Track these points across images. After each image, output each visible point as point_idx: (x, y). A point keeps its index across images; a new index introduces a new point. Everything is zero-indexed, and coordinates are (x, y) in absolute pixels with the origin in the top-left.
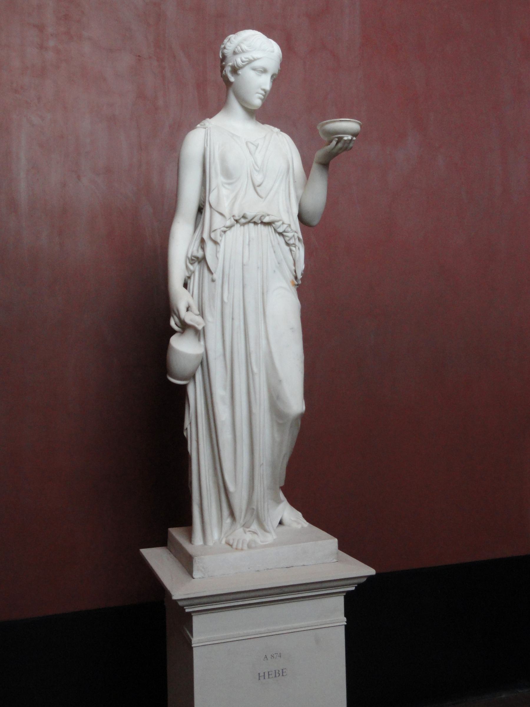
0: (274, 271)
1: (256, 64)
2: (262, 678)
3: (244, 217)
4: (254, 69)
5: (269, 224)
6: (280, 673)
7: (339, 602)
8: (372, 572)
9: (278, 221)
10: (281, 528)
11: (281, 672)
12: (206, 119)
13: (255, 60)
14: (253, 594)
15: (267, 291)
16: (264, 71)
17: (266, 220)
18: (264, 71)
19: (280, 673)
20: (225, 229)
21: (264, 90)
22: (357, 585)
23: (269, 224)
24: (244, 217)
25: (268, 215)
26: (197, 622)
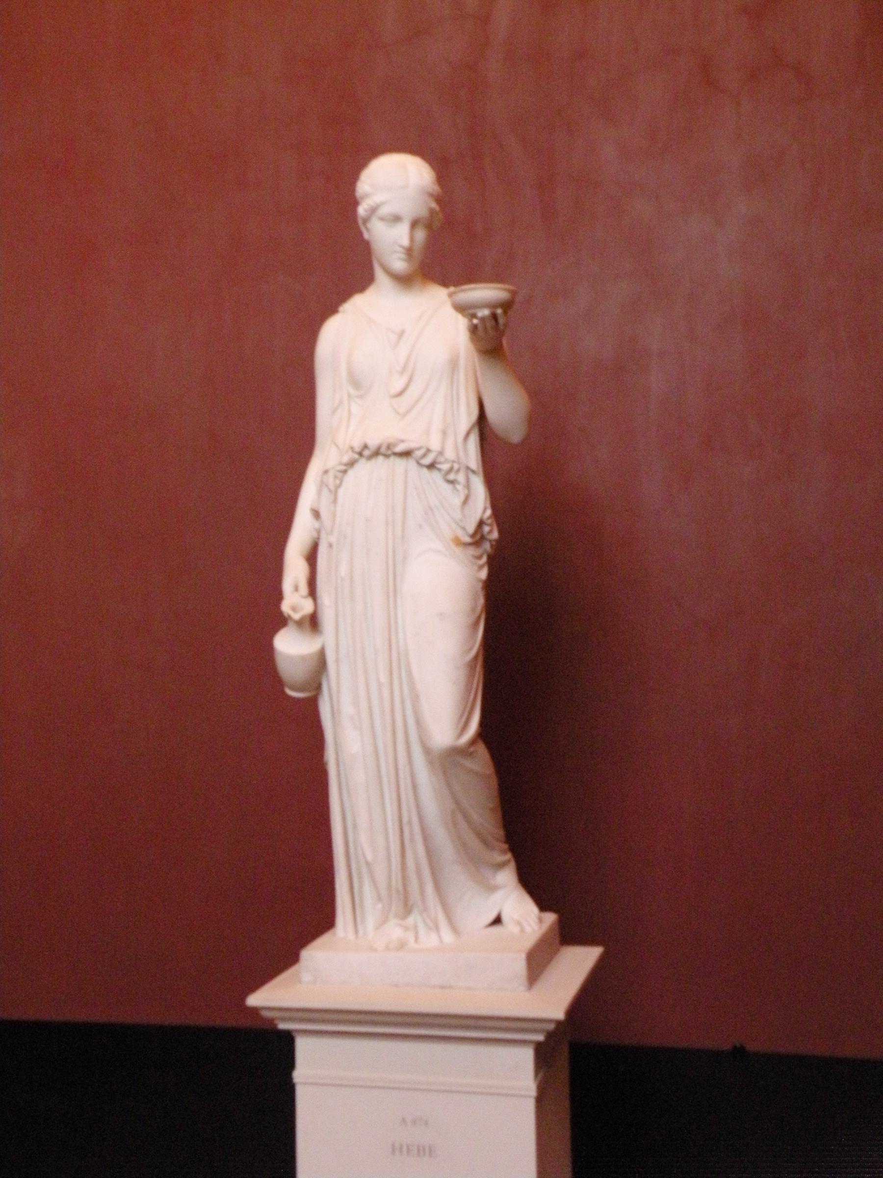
0: (420, 526)
1: (384, 211)
2: (397, 1153)
3: (366, 447)
4: (382, 219)
5: (407, 454)
6: (425, 1151)
7: (526, 1057)
8: (254, 1000)
9: (419, 449)
10: (496, 929)
11: (427, 1150)
12: (341, 309)
13: (382, 204)
14: (300, 1015)
15: (405, 558)
16: (396, 219)
17: (400, 448)
18: (396, 219)
19: (425, 1151)
20: (343, 468)
21: (401, 246)
22: (541, 1038)
23: (407, 454)
24: (366, 447)
25: (403, 441)
26: (303, 1047)
